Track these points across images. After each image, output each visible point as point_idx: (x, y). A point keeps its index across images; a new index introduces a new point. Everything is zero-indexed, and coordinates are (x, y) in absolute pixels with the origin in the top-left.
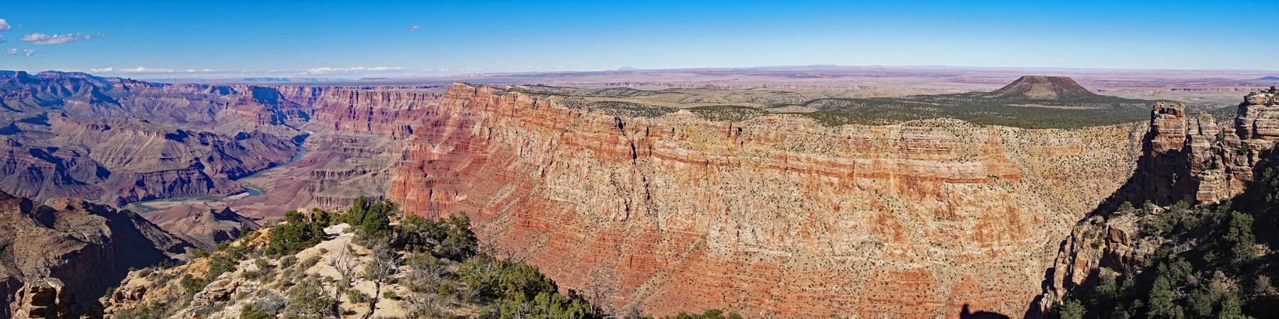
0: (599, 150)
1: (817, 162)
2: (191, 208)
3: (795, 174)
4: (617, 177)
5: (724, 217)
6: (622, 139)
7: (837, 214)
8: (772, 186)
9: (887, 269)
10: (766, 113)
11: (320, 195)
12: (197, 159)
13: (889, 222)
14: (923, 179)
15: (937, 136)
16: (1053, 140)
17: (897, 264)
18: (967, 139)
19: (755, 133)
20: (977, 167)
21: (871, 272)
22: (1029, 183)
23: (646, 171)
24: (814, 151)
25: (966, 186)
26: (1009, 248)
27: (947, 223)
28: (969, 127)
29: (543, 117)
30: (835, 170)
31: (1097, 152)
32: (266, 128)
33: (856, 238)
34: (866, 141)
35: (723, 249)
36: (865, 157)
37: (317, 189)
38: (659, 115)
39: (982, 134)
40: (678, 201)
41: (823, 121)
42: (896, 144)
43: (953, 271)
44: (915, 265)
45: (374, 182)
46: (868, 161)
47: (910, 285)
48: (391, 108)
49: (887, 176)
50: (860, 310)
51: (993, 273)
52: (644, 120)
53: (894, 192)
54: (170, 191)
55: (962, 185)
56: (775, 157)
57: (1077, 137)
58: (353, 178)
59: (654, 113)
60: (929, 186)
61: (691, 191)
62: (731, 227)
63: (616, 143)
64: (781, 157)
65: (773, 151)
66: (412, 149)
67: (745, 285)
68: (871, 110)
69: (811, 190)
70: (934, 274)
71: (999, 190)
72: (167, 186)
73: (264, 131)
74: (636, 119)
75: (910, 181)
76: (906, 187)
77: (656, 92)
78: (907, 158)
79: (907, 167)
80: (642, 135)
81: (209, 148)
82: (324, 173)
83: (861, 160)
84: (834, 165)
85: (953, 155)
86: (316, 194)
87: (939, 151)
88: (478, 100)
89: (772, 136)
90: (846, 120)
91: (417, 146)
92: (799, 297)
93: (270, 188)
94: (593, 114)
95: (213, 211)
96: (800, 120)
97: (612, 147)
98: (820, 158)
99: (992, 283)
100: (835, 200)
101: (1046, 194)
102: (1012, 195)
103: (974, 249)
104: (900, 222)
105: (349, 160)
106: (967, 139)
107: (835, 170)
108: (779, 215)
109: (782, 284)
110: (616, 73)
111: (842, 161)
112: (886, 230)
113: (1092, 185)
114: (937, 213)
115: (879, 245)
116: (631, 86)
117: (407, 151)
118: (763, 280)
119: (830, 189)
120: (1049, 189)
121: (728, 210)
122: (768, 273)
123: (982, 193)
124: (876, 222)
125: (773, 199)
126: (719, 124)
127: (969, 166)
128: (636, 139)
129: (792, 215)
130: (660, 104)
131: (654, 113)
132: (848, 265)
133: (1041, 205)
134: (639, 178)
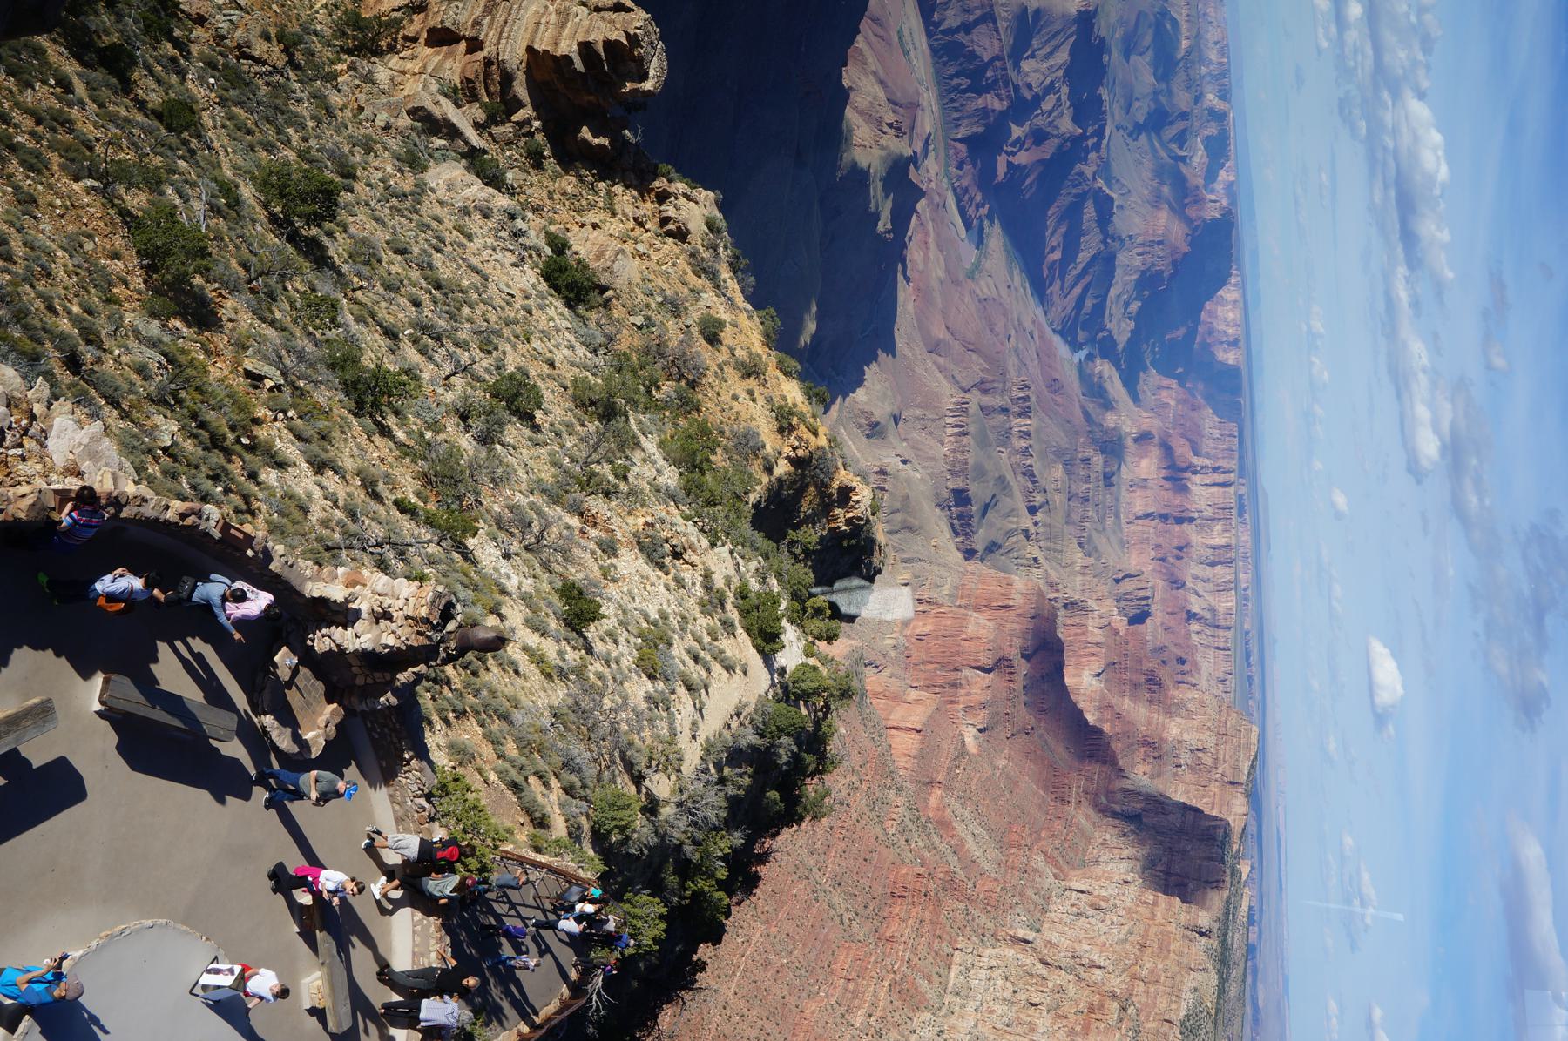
2: (914, 107)
11: (973, 408)
12: (1038, 100)
29: (1164, 949)
32: (1129, 263)
37: (987, 400)
45: (1009, 534)
48: (1192, 570)
54: (949, 51)
58: (1017, 484)
66: (1092, 623)
72: (961, 37)
73: (1122, 258)
81: (1066, 125)
82: (1026, 412)
86: (975, 398)
88: (1214, 788)
91: (1098, 636)
93: (985, 287)
95: (913, 160)
105: (1058, 472)
117: (1085, 610)
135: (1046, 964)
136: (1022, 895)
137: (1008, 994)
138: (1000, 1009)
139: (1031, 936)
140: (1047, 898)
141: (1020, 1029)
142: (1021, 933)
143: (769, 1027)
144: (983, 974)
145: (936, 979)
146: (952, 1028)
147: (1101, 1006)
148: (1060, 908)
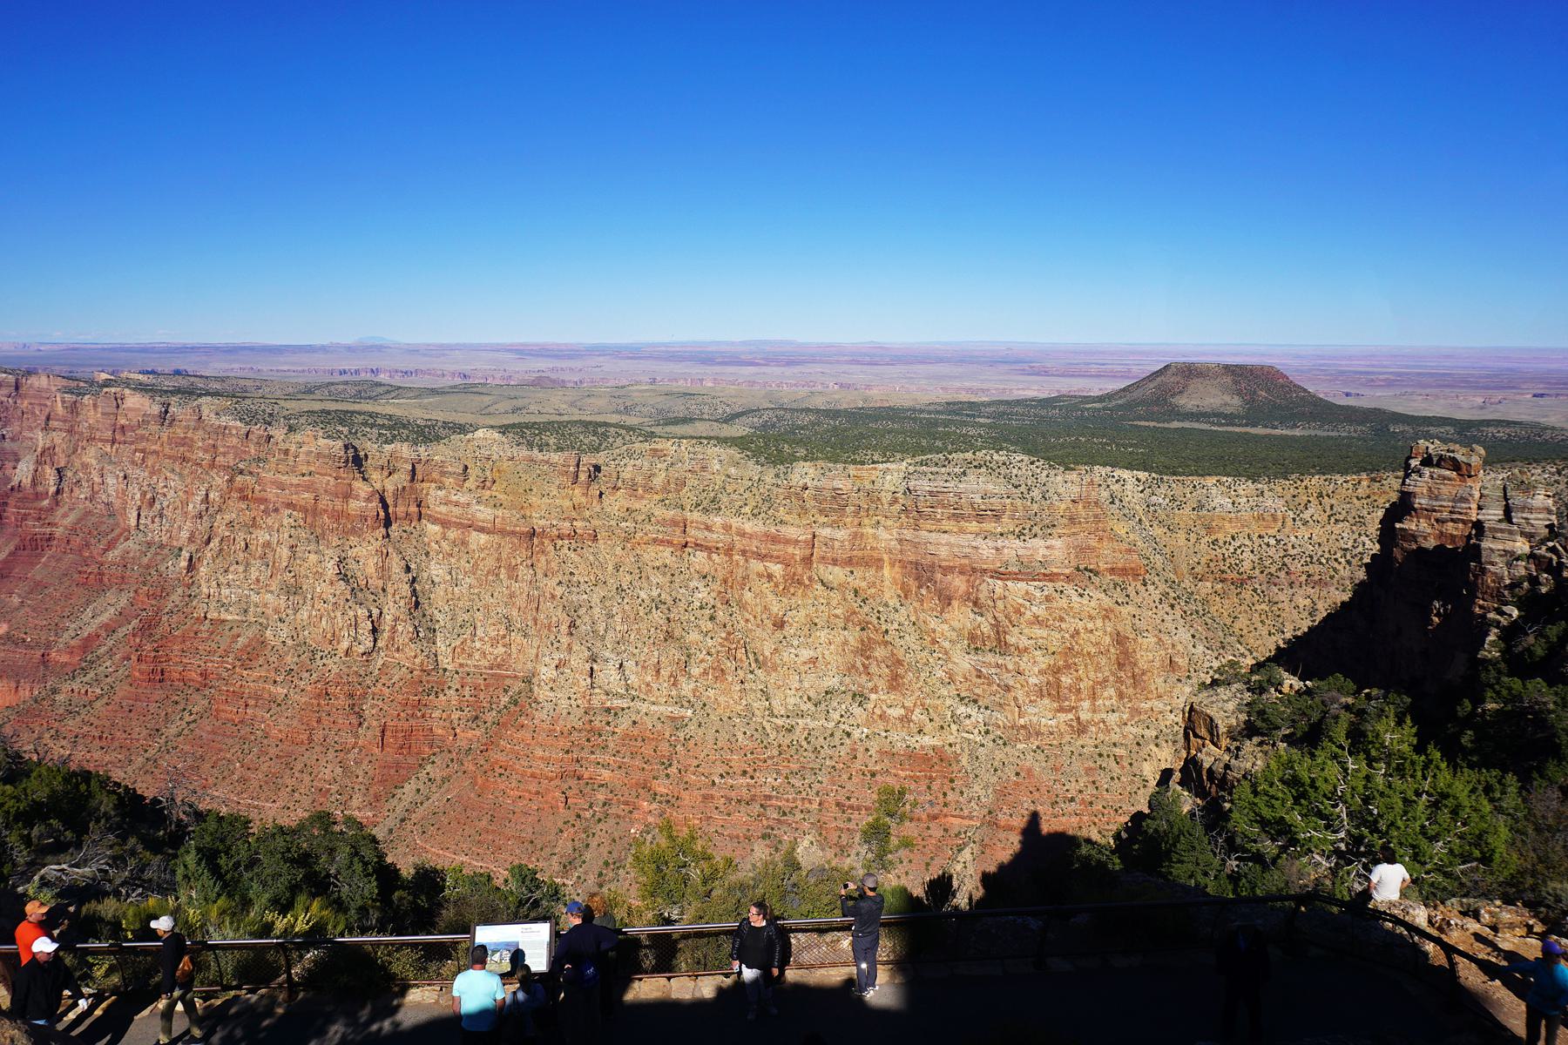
0: (311, 512)
1: (742, 534)
3: (701, 556)
4: (352, 565)
5: (565, 640)
6: (361, 488)
7: (779, 635)
8: (656, 578)
9: (874, 747)
10: (650, 436)
13: (880, 652)
14: (947, 570)
15: (977, 486)
16: (1220, 500)
17: (894, 736)
18: (1036, 493)
19: (626, 475)
20: (1053, 550)
21: (843, 751)
22: (1163, 587)
23: (411, 551)
24: (738, 513)
25: (1031, 587)
26: (1113, 719)
27: (990, 658)
28: (1041, 469)
30: (777, 549)
31: (1317, 531)
33: (814, 684)
34: (837, 494)
35: (564, 703)
36: (835, 525)
38: (438, 438)
39: (1066, 485)
40: (478, 611)
41: (756, 454)
42: (896, 501)
43: (999, 755)
44: (927, 741)
46: (841, 534)
47: (916, 780)
49: (878, 563)
50: (820, 826)
51: (1078, 766)
52: (405, 450)
53: (890, 595)
55: (1022, 585)
56: (663, 523)
57: (1275, 497)
59: (425, 434)
60: (959, 583)
61: (501, 590)
62: (578, 660)
63: (348, 495)
64: (674, 523)
65: (659, 512)
67: (606, 774)
68: (851, 433)
69: (729, 589)
70: (964, 761)
71: (1097, 598)
74: (388, 447)
75: (923, 575)
76: (913, 584)
77: (434, 392)
78: (917, 528)
79: (916, 545)
80: (401, 478)
83: (826, 532)
84: (775, 539)
85: (1007, 524)
87: (980, 517)
89: (658, 481)
90: (802, 452)
92: (705, 798)
94: (298, 437)
96: (713, 450)
97: (338, 504)
98: (748, 527)
99: (1073, 787)
100: (776, 609)
101: (1197, 613)
102: (1125, 610)
103: (1042, 714)
104: (900, 654)
106: (1036, 493)
107: (777, 549)
108: (669, 636)
109: (673, 770)
110: (350, 349)
111: (791, 532)
112: (873, 669)
113: (1302, 602)
114: (972, 637)
115: (860, 697)
116: (383, 377)
118: (638, 762)
119: (766, 587)
120: (1205, 601)
121: (573, 625)
122: (647, 750)
123: (1063, 603)
124: (856, 652)
125: (658, 603)
126: (555, 457)
127: (1038, 548)
128: (390, 487)
129: (694, 636)
130: (440, 416)
131: (425, 434)
132: (799, 735)
133: (1184, 635)
134: (396, 565)
135: (209, 541)
136: (148, 567)
137: (241, 568)
138: (254, 574)
139: (185, 554)
140: (149, 545)
141: (270, 556)
142: (184, 564)
143: (299, 766)
144: (225, 591)
145: (235, 630)
146: (277, 611)
147: (241, 490)
148: (157, 533)
